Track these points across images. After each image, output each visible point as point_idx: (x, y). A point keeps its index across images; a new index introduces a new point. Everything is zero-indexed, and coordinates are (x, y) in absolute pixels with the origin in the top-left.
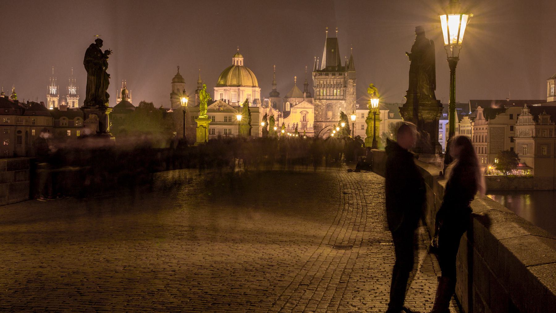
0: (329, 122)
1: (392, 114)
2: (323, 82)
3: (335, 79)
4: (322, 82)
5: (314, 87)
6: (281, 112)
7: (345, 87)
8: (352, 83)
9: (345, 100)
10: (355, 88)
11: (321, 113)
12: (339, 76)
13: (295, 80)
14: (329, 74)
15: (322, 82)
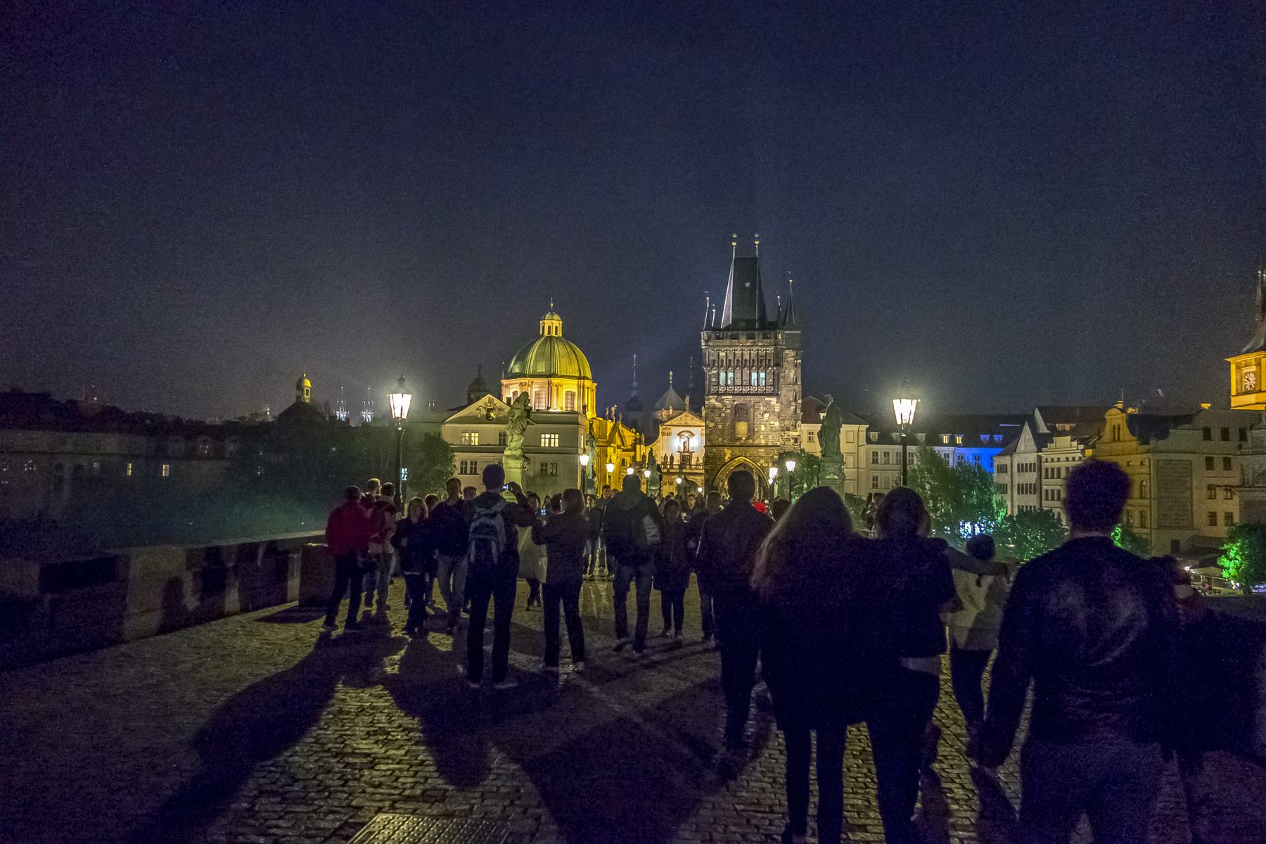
0: (739, 446)
1: (874, 433)
2: (726, 353)
3: (755, 348)
4: (722, 354)
5: (706, 366)
6: (640, 434)
7: (778, 365)
8: (793, 359)
9: (777, 395)
10: (799, 370)
11: (720, 427)
12: (765, 340)
13: (671, 378)
14: (740, 337)
15: (724, 354)
